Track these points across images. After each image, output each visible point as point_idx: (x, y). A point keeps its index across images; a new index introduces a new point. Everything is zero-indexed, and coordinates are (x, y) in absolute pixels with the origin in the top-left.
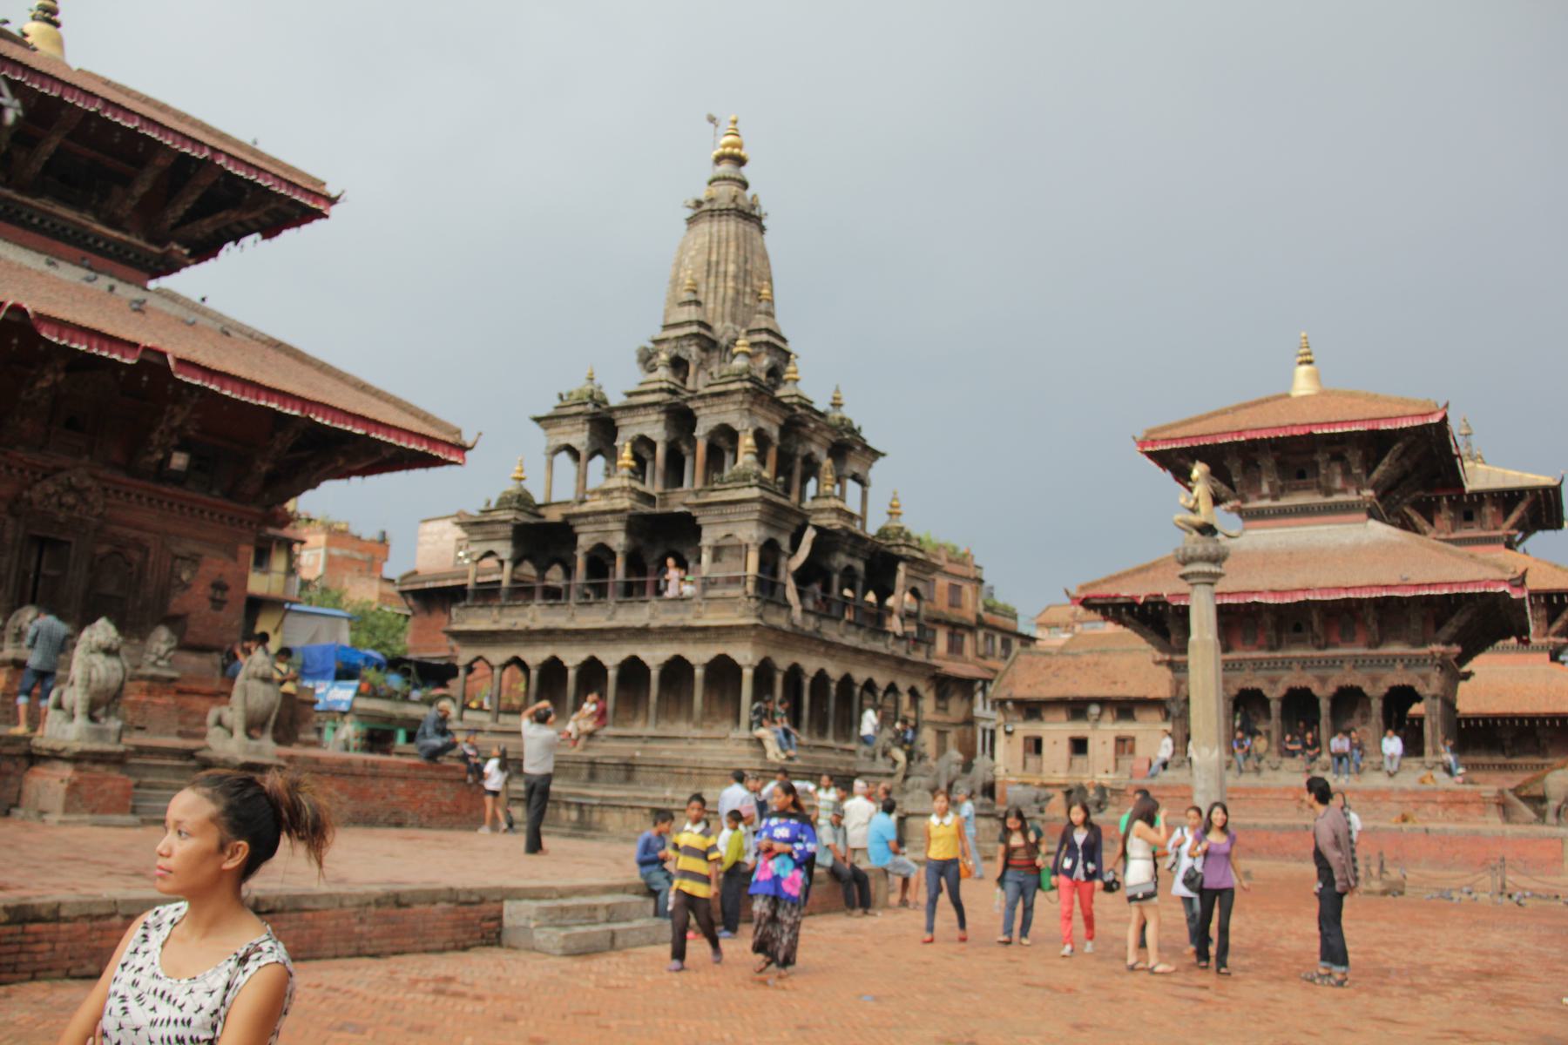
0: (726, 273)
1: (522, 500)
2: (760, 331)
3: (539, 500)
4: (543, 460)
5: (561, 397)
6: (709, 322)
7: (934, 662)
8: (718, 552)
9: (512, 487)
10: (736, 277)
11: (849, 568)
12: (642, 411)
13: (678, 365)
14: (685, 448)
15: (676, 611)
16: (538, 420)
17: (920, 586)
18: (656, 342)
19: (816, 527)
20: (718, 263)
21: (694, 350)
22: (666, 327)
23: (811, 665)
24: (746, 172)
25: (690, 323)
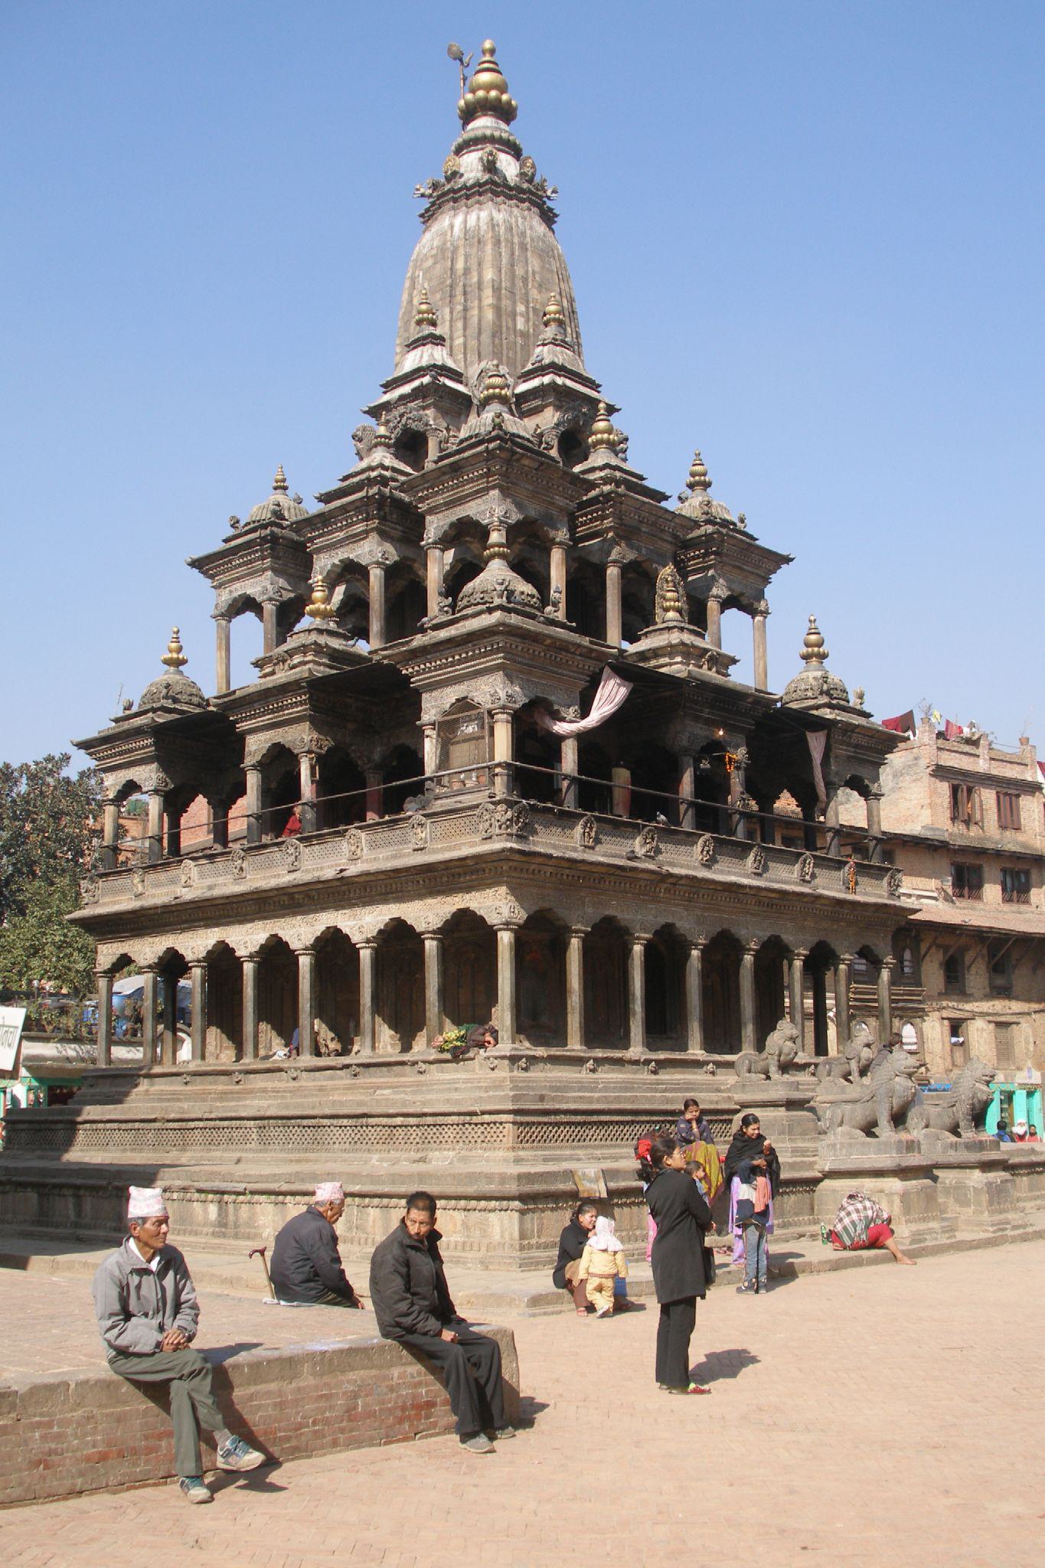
0: (480, 284)
2: (541, 370)
6: (459, 367)
7: (905, 902)
9: (162, 674)
10: (497, 290)
13: (410, 445)
16: (198, 564)
18: (375, 412)
20: (467, 271)
21: (430, 413)
22: (388, 386)
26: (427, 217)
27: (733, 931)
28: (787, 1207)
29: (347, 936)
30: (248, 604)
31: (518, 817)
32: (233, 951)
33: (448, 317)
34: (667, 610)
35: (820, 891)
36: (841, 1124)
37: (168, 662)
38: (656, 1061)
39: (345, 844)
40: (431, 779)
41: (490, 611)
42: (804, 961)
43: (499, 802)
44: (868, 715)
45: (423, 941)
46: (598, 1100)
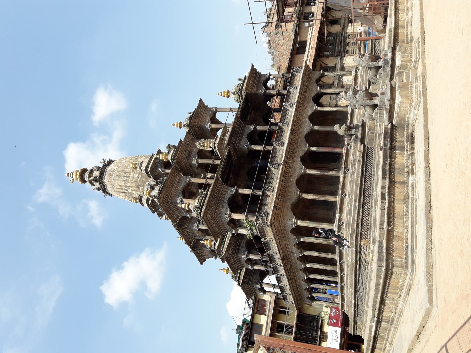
2: (147, 173)
16: (202, 263)
17: (263, 79)
20: (122, 189)
27: (305, 134)
28: (401, 139)
31: (262, 217)
35: (296, 101)
36: (372, 116)
37: (227, 273)
38: (345, 169)
42: (318, 106)
44: (245, 77)
45: (301, 242)
46: (355, 203)
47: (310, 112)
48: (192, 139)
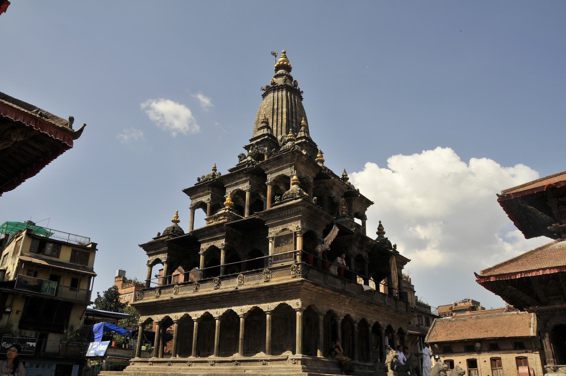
1: (176, 231)
2: (301, 138)
3: (187, 230)
4: (189, 211)
5: (199, 179)
8: (279, 241)
11: (359, 256)
12: (238, 176)
13: (258, 157)
14: (262, 196)
15: (254, 280)
18: (247, 148)
19: (339, 226)
22: (251, 140)
23: (341, 311)
24: (291, 74)
25: (263, 135)
26: (264, 96)
29: (235, 313)
30: (202, 205)
32: (191, 317)
33: (271, 121)
34: (342, 212)
37: (173, 221)
39: (237, 279)
40: (271, 257)
41: (296, 199)
43: (299, 264)
47: (381, 323)
48: (343, 191)
